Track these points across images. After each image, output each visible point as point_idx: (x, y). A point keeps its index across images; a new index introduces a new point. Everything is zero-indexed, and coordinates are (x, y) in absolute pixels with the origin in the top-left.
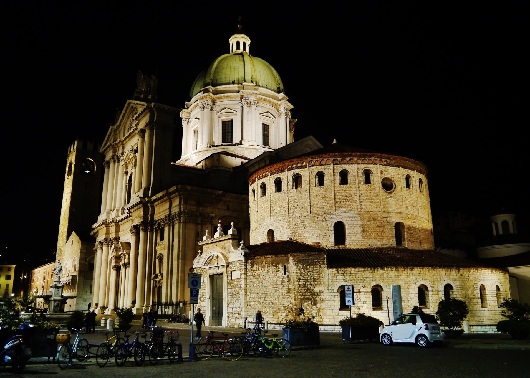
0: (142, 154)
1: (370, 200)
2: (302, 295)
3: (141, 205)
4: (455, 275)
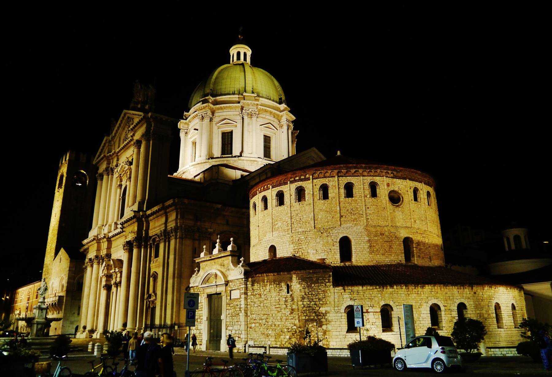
0: (138, 166)
1: (377, 214)
2: (307, 316)
3: (134, 220)
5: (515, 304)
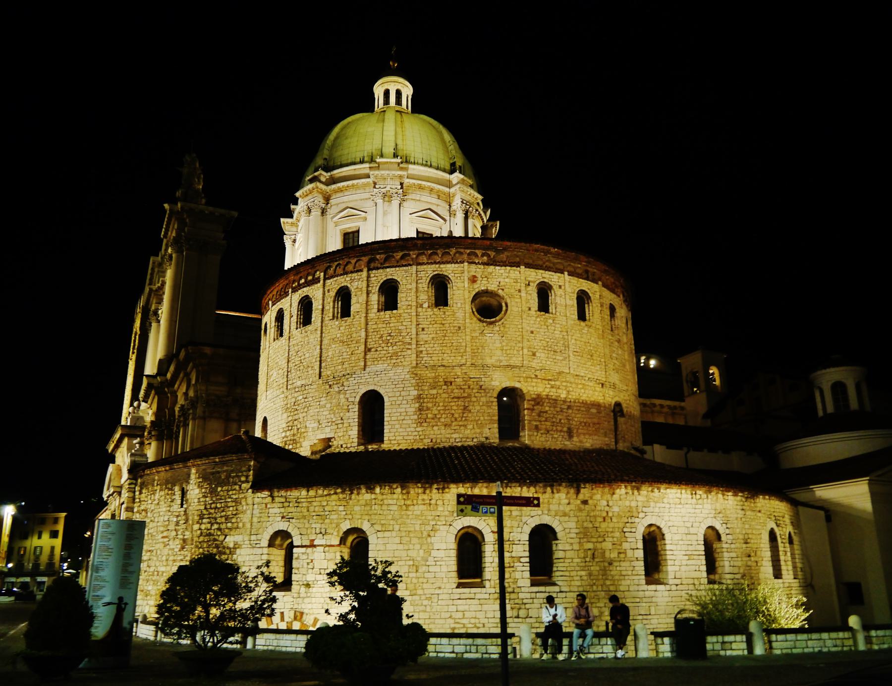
1: (441, 342)
4: (567, 501)
5: (718, 527)
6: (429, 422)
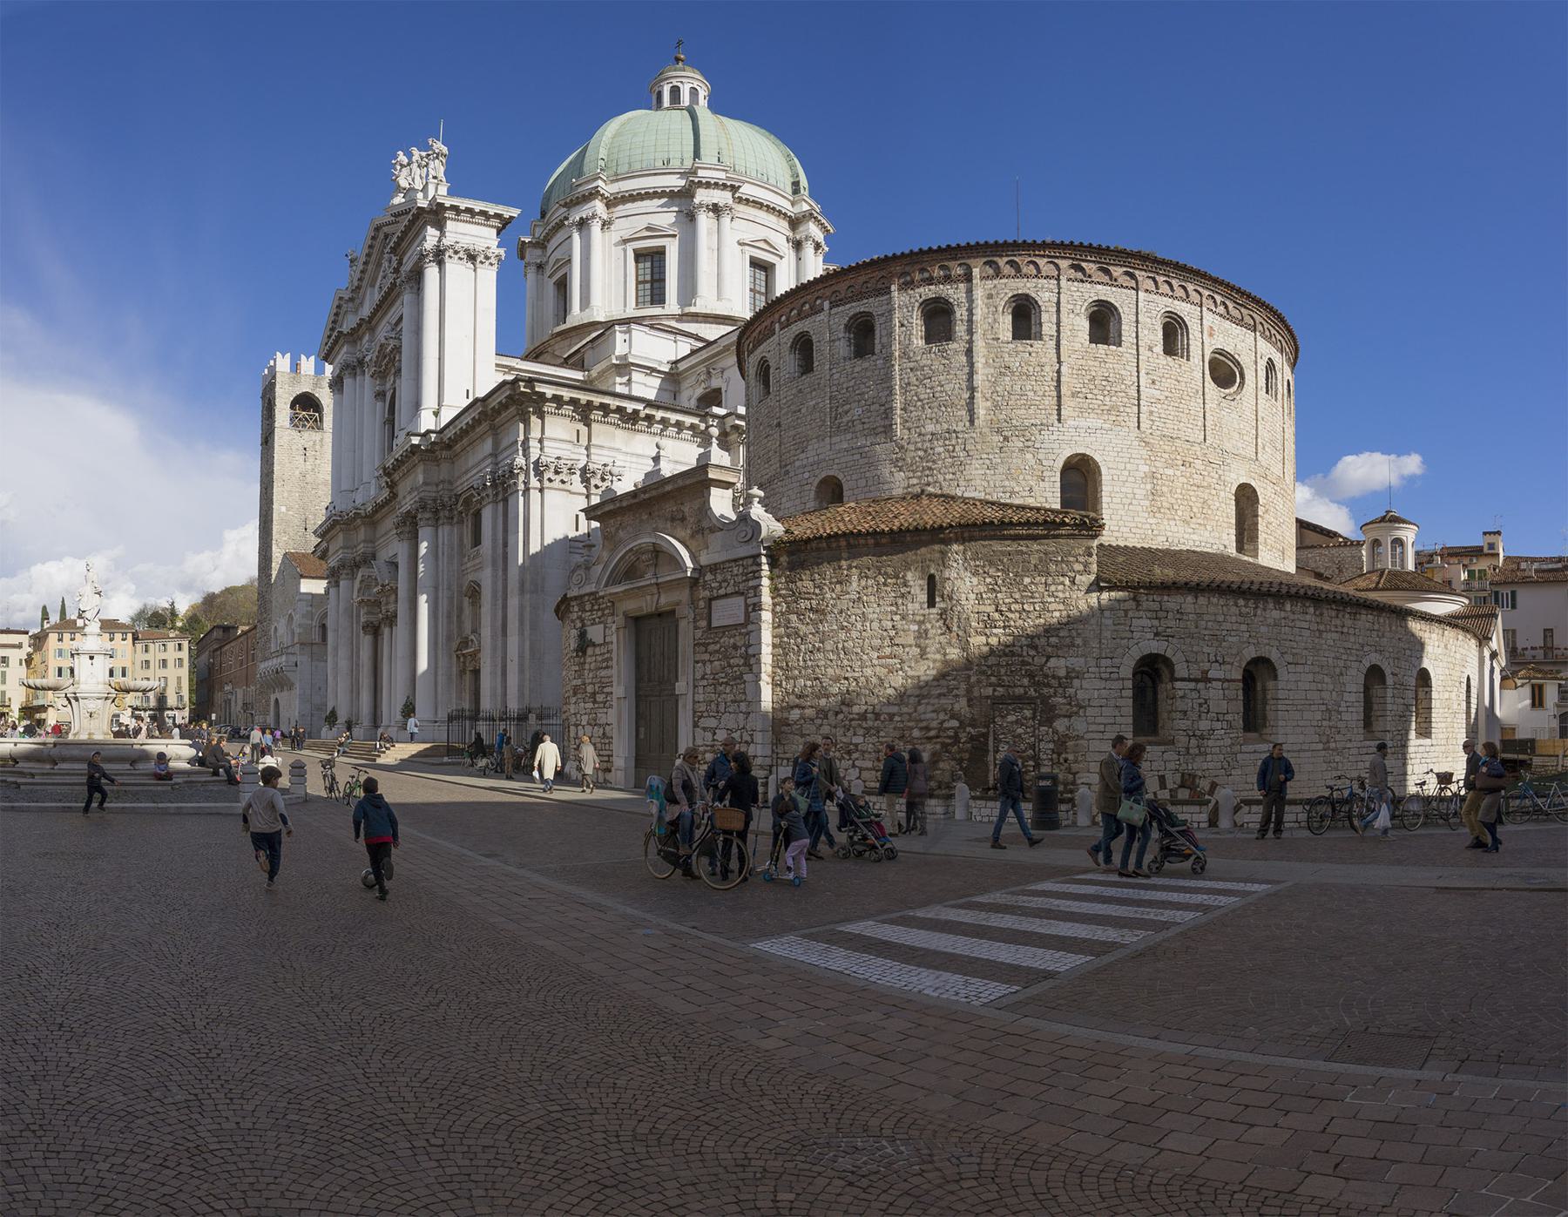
6: (1164, 513)
